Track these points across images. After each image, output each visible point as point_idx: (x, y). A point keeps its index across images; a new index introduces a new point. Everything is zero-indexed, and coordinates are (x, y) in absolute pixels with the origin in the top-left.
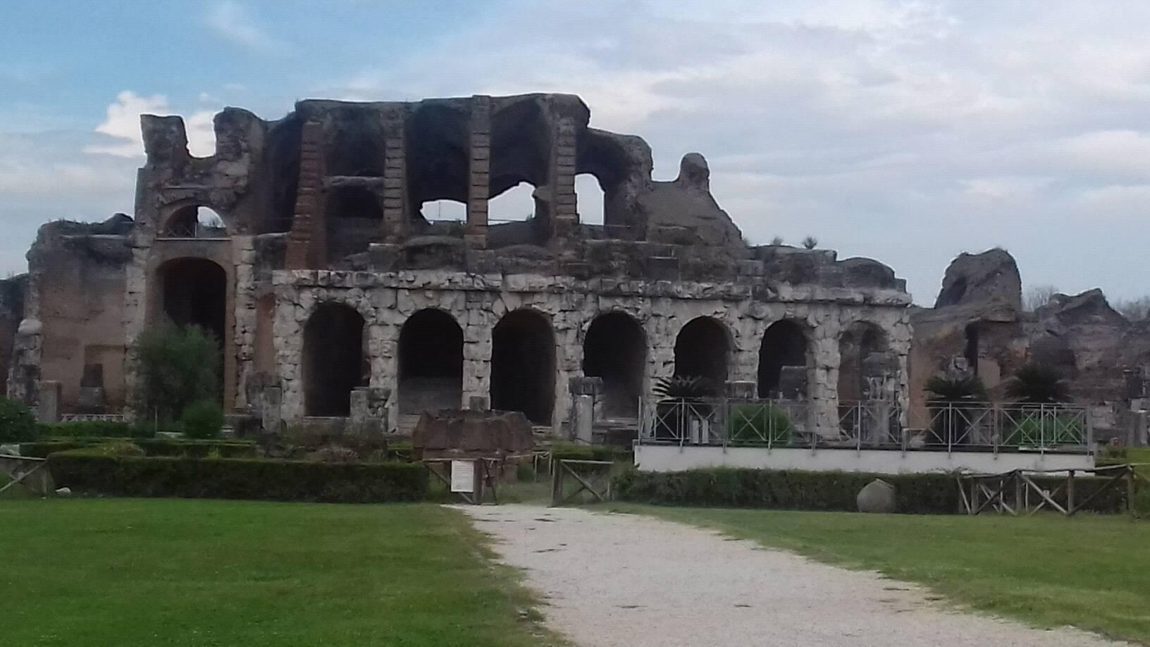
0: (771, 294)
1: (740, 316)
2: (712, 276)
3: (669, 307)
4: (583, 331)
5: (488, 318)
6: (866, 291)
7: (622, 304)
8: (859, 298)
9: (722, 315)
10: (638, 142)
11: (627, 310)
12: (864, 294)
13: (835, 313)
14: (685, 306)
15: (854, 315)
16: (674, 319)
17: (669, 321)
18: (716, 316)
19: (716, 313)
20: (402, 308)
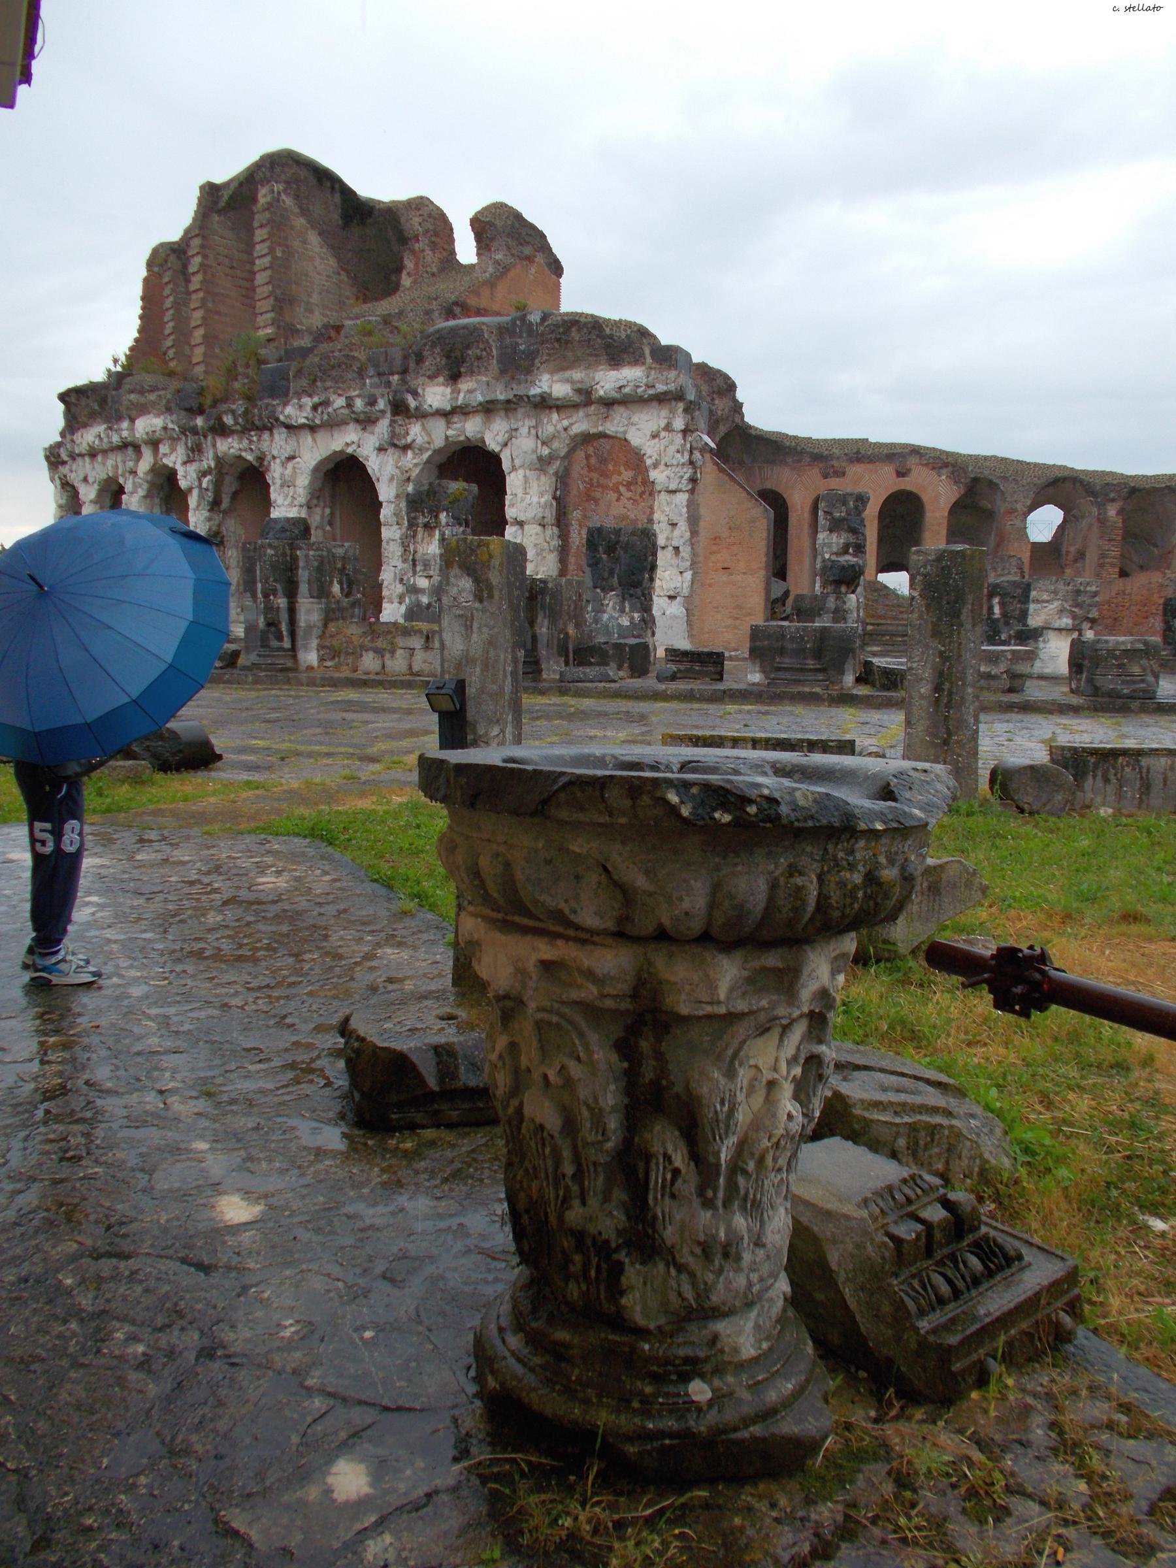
0: (412, 403)
1: (377, 445)
2: (329, 384)
3: (282, 443)
4: (207, 489)
5: (134, 483)
6: (577, 375)
7: (236, 445)
8: (560, 389)
9: (354, 447)
10: (421, 205)
11: (243, 454)
12: (572, 382)
13: (525, 425)
14: (307, 439)
15: (565, 423)
16: (298, 460)
17: (290, 465)
18: (350, 450)
19: (347, 445)
20: (91, 480)
